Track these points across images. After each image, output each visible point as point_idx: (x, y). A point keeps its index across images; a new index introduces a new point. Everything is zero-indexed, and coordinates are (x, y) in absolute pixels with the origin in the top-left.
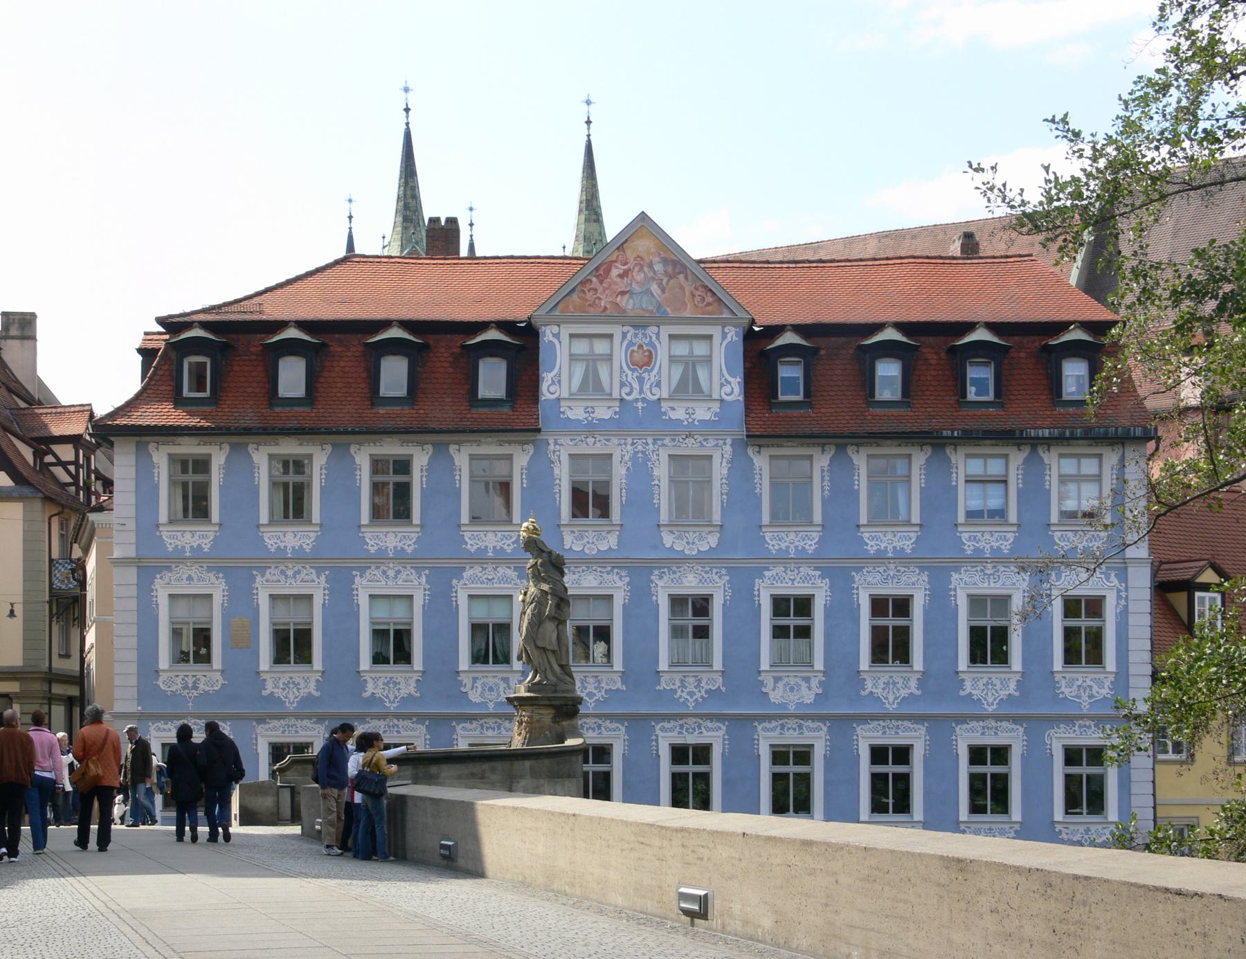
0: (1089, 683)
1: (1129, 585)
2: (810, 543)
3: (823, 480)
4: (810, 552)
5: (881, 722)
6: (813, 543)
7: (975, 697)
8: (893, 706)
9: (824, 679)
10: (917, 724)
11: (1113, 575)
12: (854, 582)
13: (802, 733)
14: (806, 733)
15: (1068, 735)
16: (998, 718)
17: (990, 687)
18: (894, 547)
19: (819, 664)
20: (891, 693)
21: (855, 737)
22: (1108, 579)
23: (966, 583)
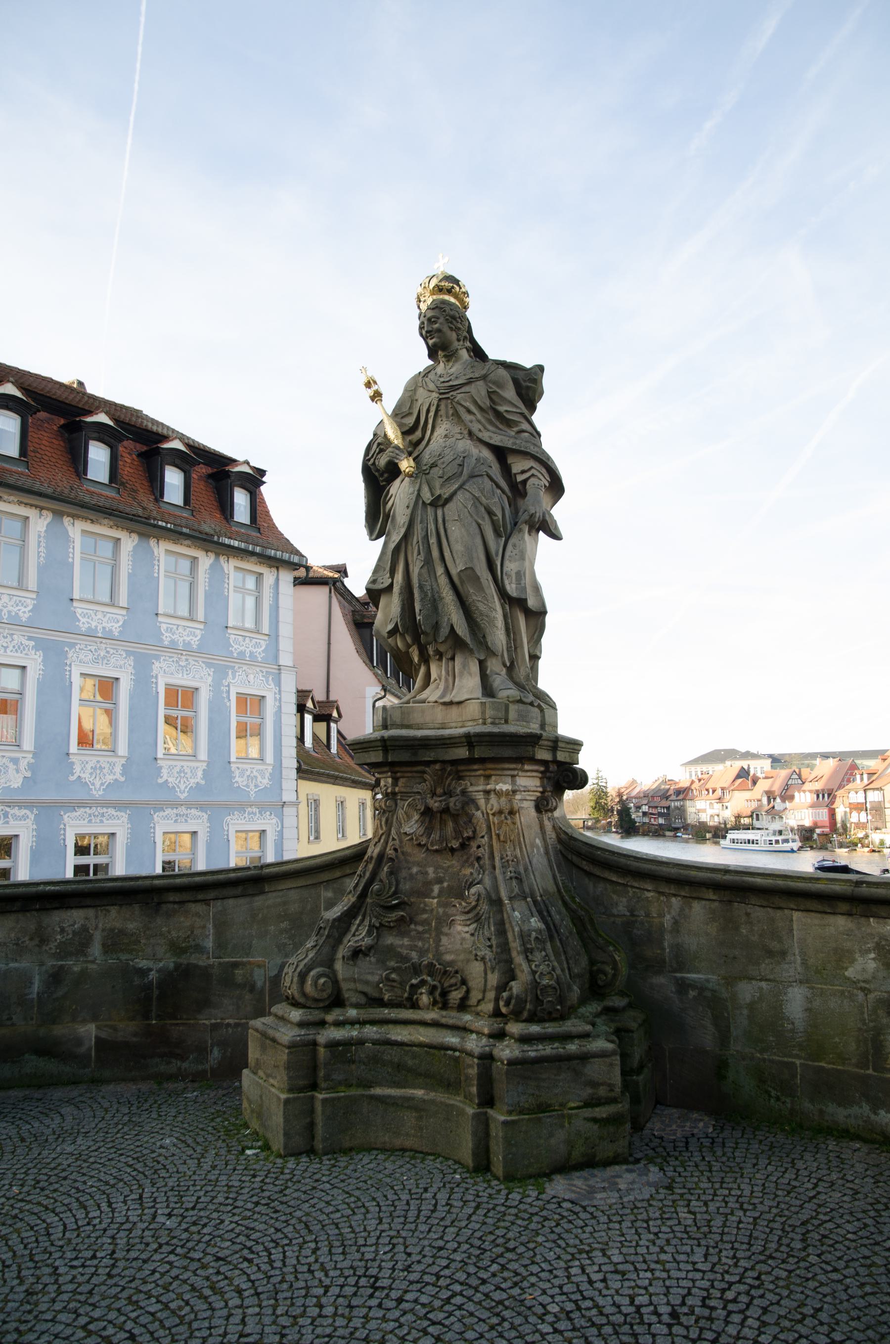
0: (255, 773)
1: (283, 689)
2: (23, 609)
3: (39, 546)
4: (24, 619)
5: (87, 810)
6: (27, 610)
7: (170, 785)
8: (101, 793)
9: (33, 761)
10: (121, 811)
11: (270, 678)
12: (67, 658)
13: (7, 823)
14: (12, 822)
15: (240, 821)
16: (189, 805)
17: (182, 775)
18: (104, 628)
19: (28, 743)
20: (98, 778)
21: (62, 826)
22: (267, 682)
23: (165, 672)
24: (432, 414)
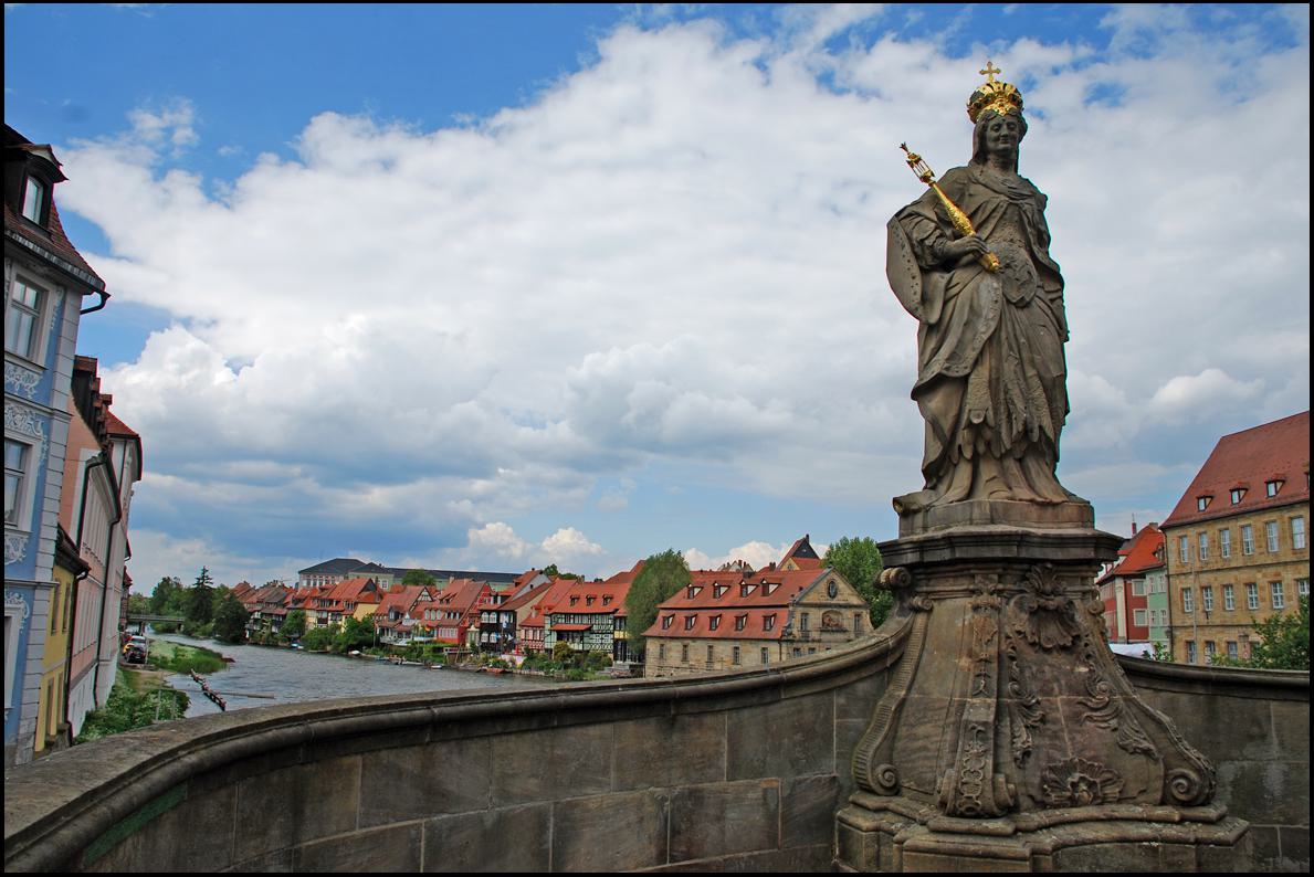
24: (998, 215)
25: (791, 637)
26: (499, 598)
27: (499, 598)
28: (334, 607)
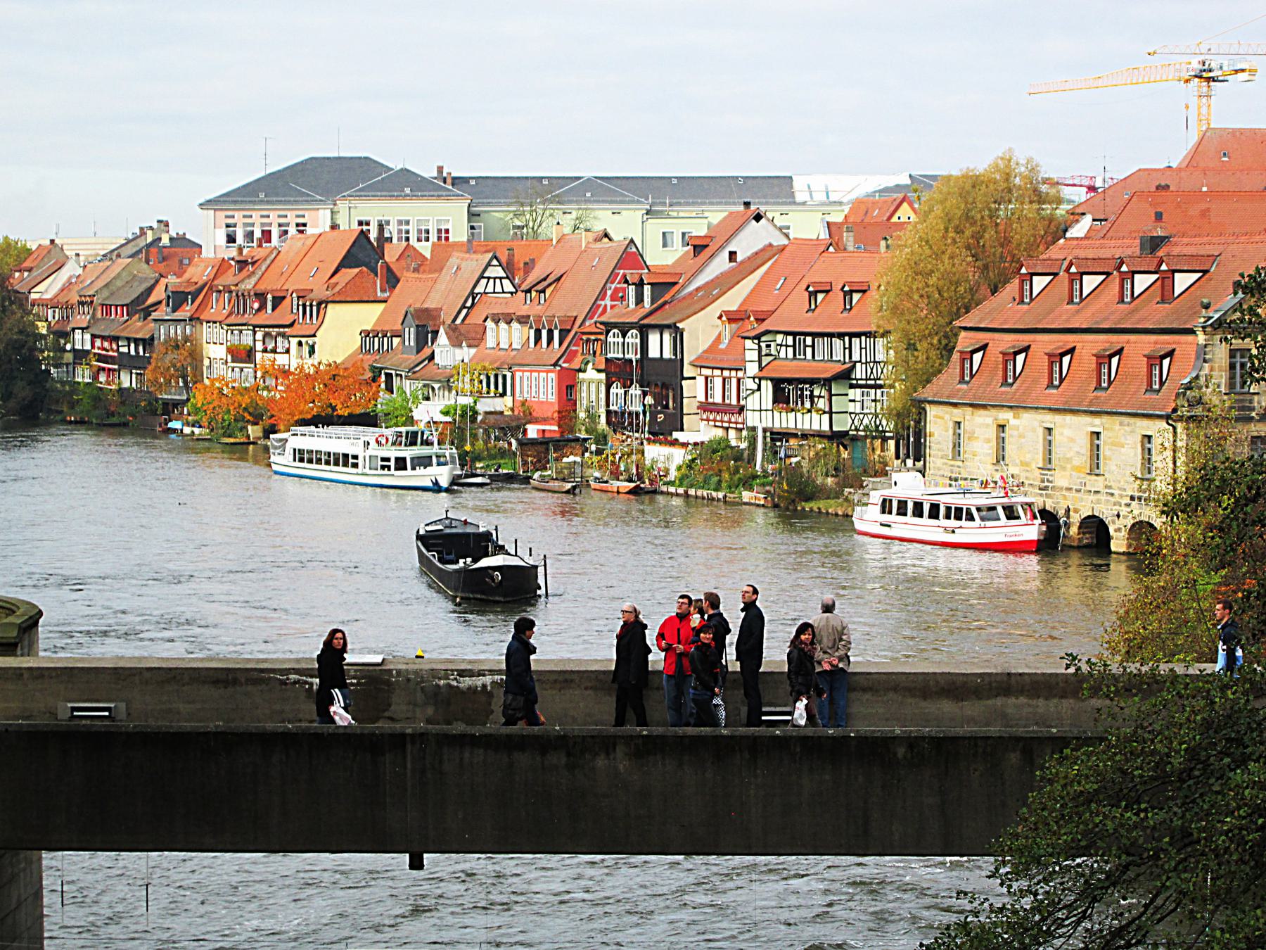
25: (1198, 411)
26: (647, 290)
27: (647, 290)
28: (268, 316)
